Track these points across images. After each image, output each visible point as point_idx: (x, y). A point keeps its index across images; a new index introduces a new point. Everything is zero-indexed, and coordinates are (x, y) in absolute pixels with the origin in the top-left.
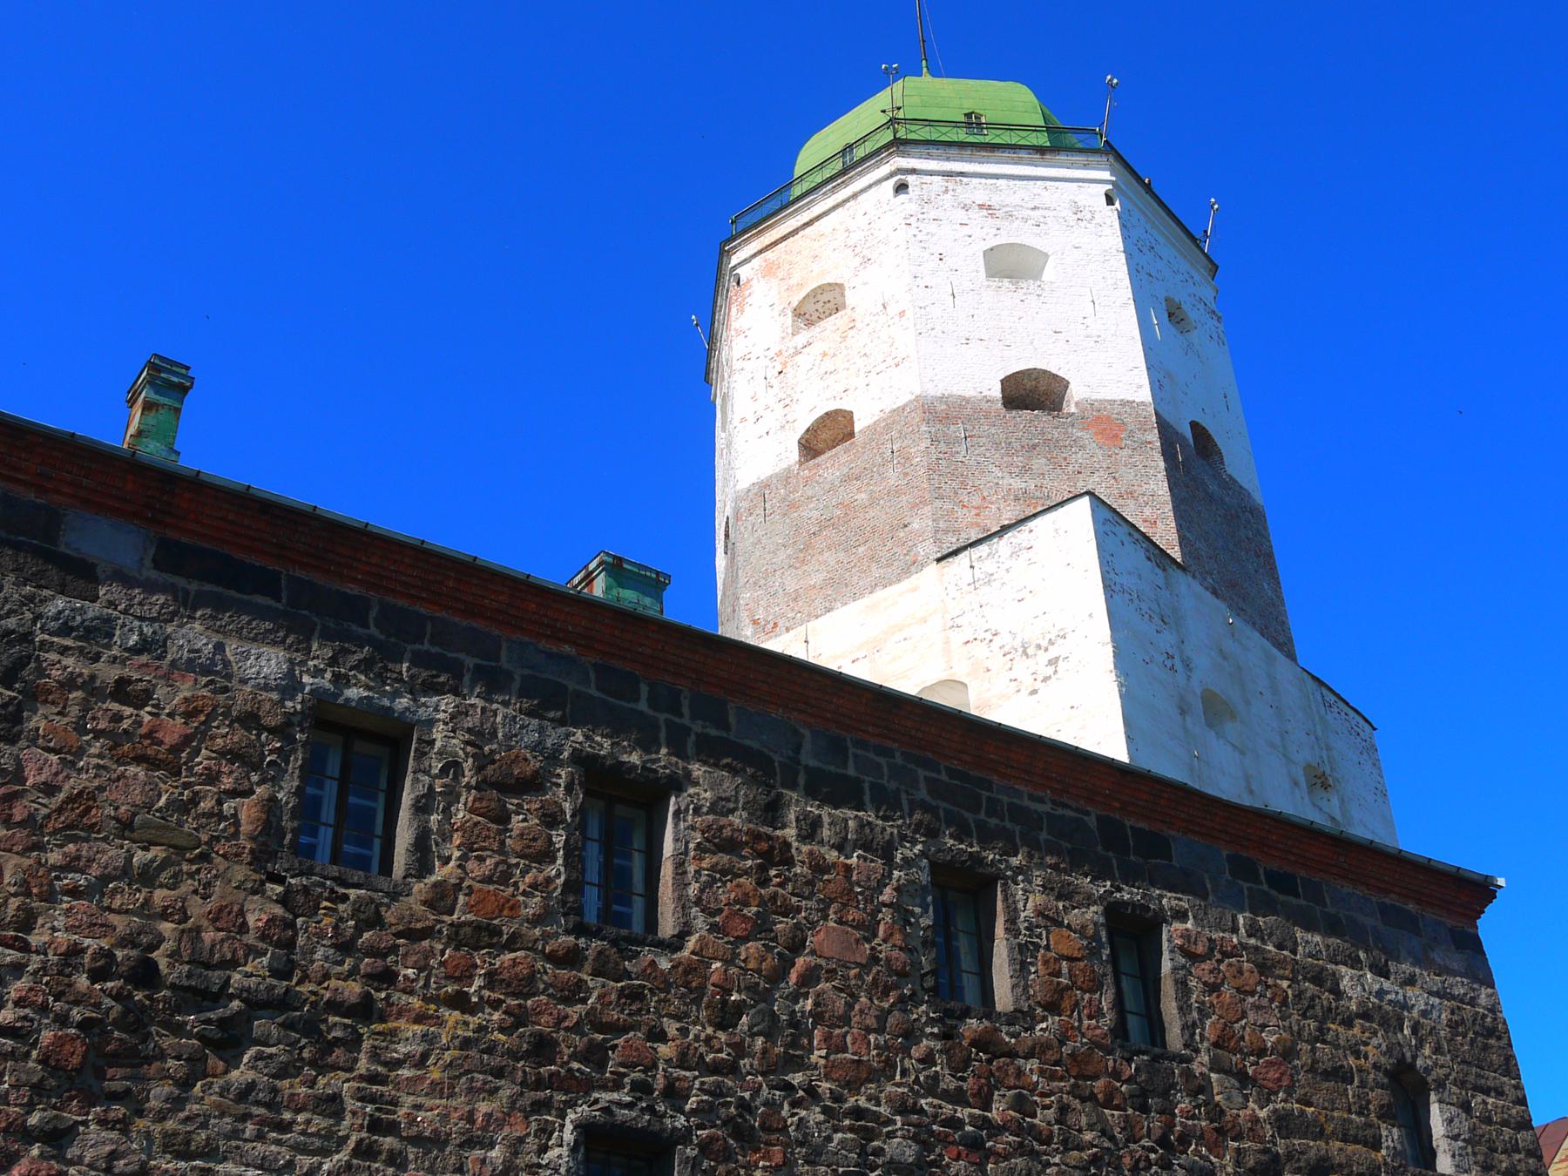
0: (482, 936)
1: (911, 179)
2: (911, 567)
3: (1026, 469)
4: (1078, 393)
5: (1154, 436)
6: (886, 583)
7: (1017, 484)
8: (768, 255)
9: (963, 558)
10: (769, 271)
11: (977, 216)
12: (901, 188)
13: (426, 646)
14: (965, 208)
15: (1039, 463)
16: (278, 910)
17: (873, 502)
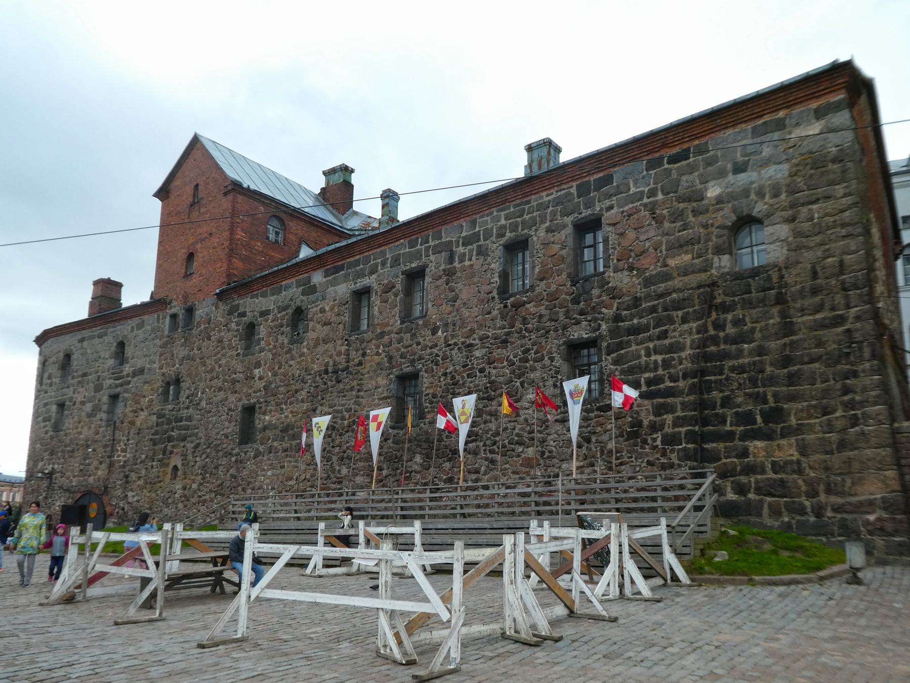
0: (382, 335)
13: (372, 262)
16: (347, 347)
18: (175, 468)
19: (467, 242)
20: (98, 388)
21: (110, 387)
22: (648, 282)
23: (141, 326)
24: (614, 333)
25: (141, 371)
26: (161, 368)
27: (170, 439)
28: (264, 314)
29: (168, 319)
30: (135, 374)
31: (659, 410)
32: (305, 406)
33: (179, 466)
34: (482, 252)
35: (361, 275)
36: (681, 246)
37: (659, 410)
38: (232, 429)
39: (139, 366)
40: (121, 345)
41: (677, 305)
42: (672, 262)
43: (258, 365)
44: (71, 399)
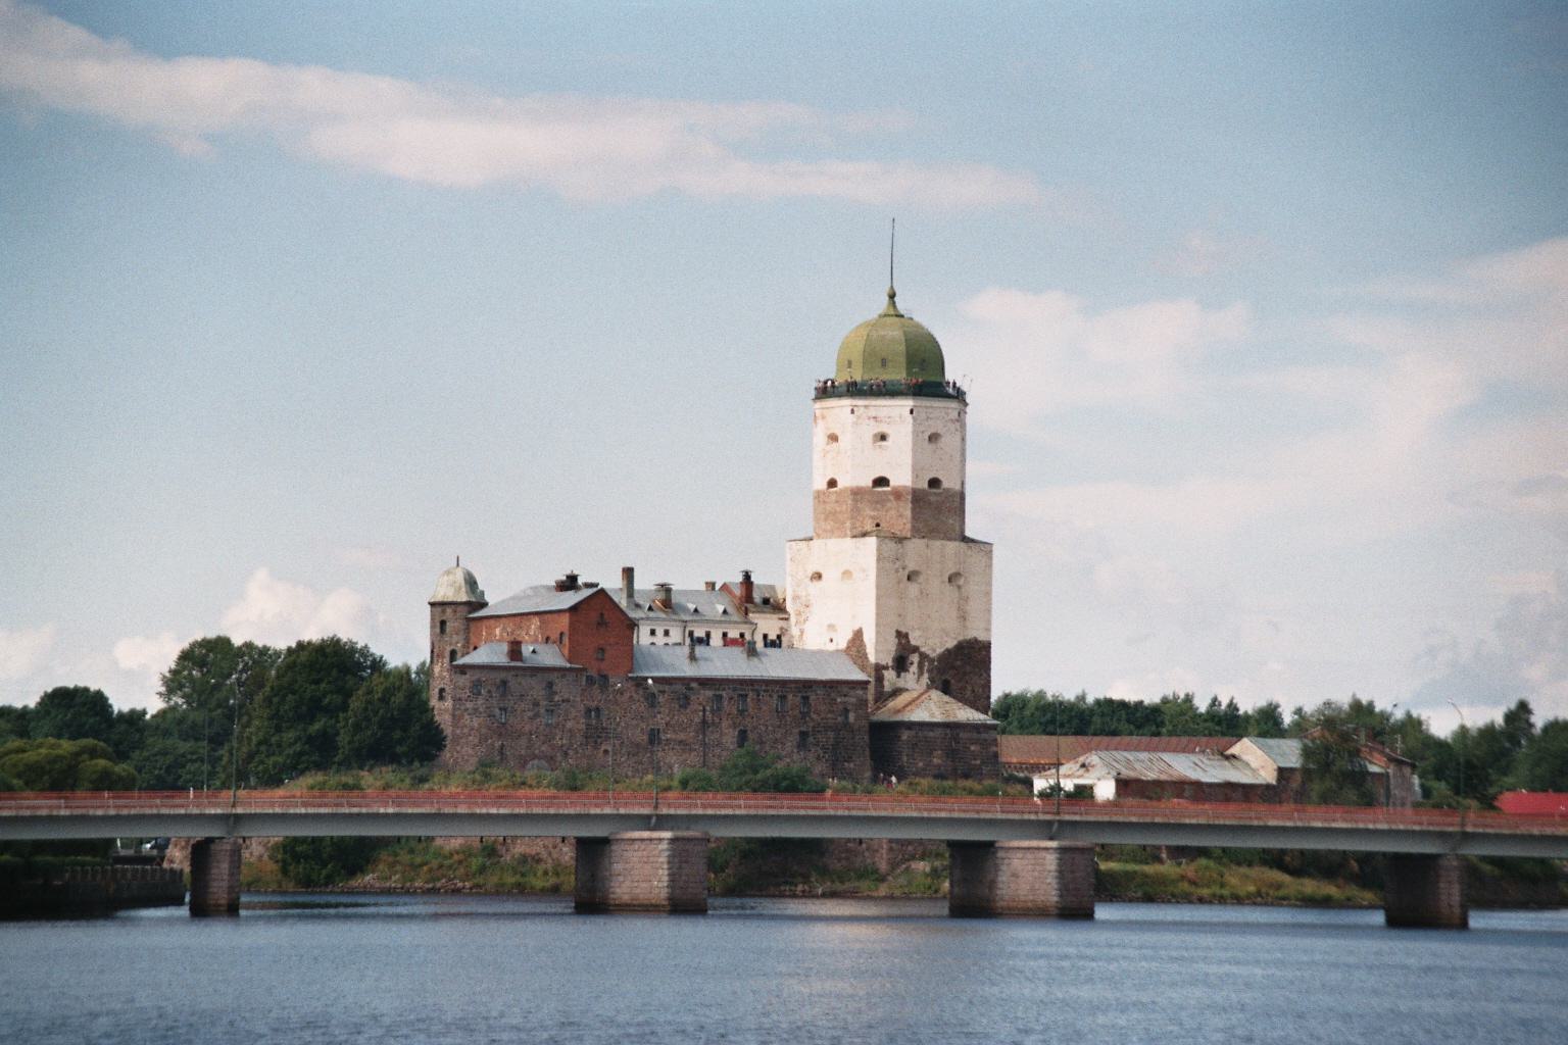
0: (729, 714)
1: (855, 409)
2: (845, 536)
3: (875, 509)
4: (891, 483)
5: (910, 497)
6: (839, 537)
7: (872, 513)
8: (825, 411)
9: (854, 539)
10: (823, 418)
11: (872, 422)
12: (853, 412)
14: (869, 418)
15: (878, 506)
17: (840, 512)
18: (606, 752)
19: (764, 691)
20: (536, 704)
21: (546, 705)
22: (822, 719)
23: (563, 676)
24: (813, 731)
25: (568, 701)
26: (582, 701)
27: (599, 737)
28: (663, 692)
29: (584, 678)
30: (563, 701)
31: (825, 753)
32: (691, 734)
33: (610, 749)
34: (771, 696)
35: (719, 690)
36: (830, 712)
37: (825, 753)
38: (645, 737)
39: (566, 697)
40: (550, 685)
41: (830, 727)
42: (829, 716)
43: (659, 713)
44: (512, 707)
